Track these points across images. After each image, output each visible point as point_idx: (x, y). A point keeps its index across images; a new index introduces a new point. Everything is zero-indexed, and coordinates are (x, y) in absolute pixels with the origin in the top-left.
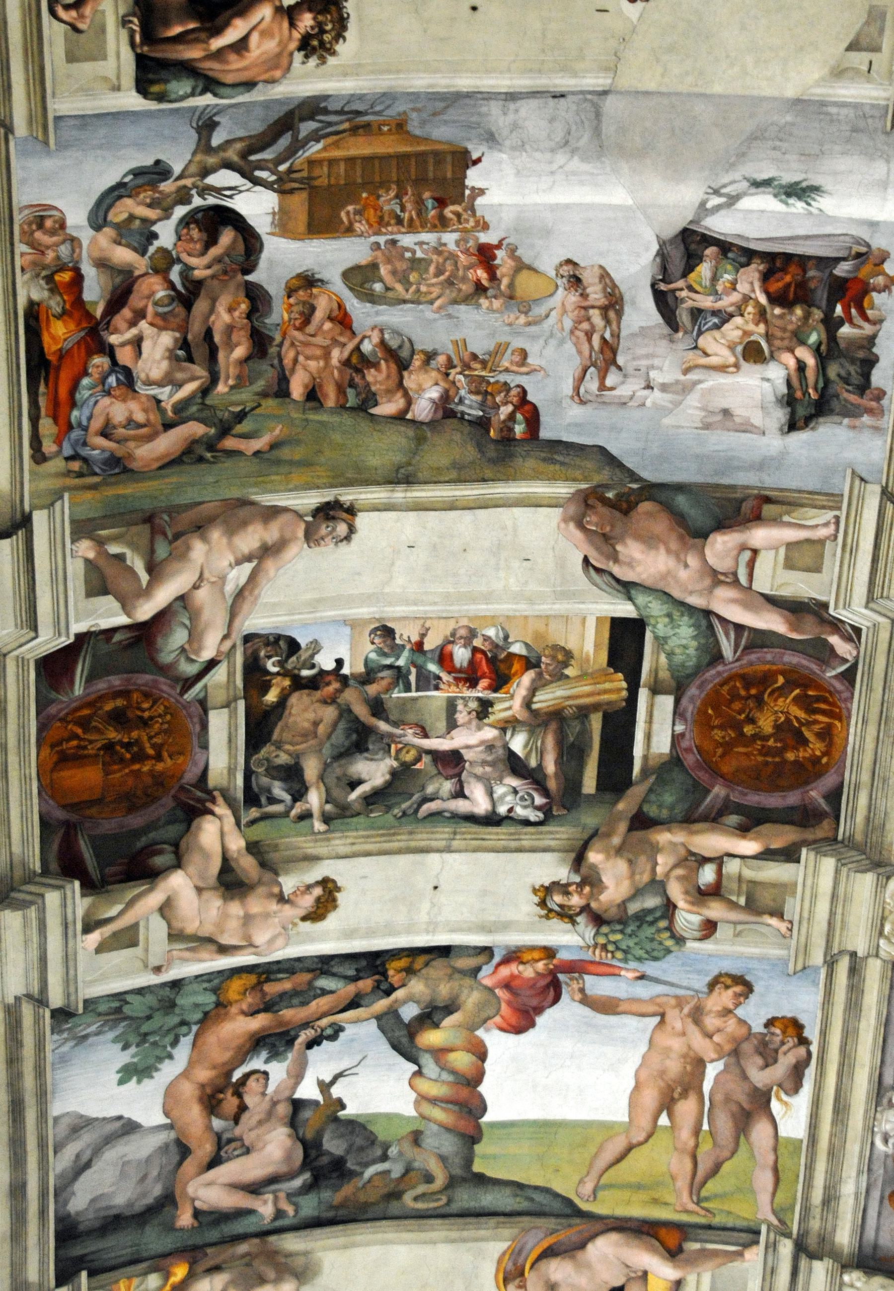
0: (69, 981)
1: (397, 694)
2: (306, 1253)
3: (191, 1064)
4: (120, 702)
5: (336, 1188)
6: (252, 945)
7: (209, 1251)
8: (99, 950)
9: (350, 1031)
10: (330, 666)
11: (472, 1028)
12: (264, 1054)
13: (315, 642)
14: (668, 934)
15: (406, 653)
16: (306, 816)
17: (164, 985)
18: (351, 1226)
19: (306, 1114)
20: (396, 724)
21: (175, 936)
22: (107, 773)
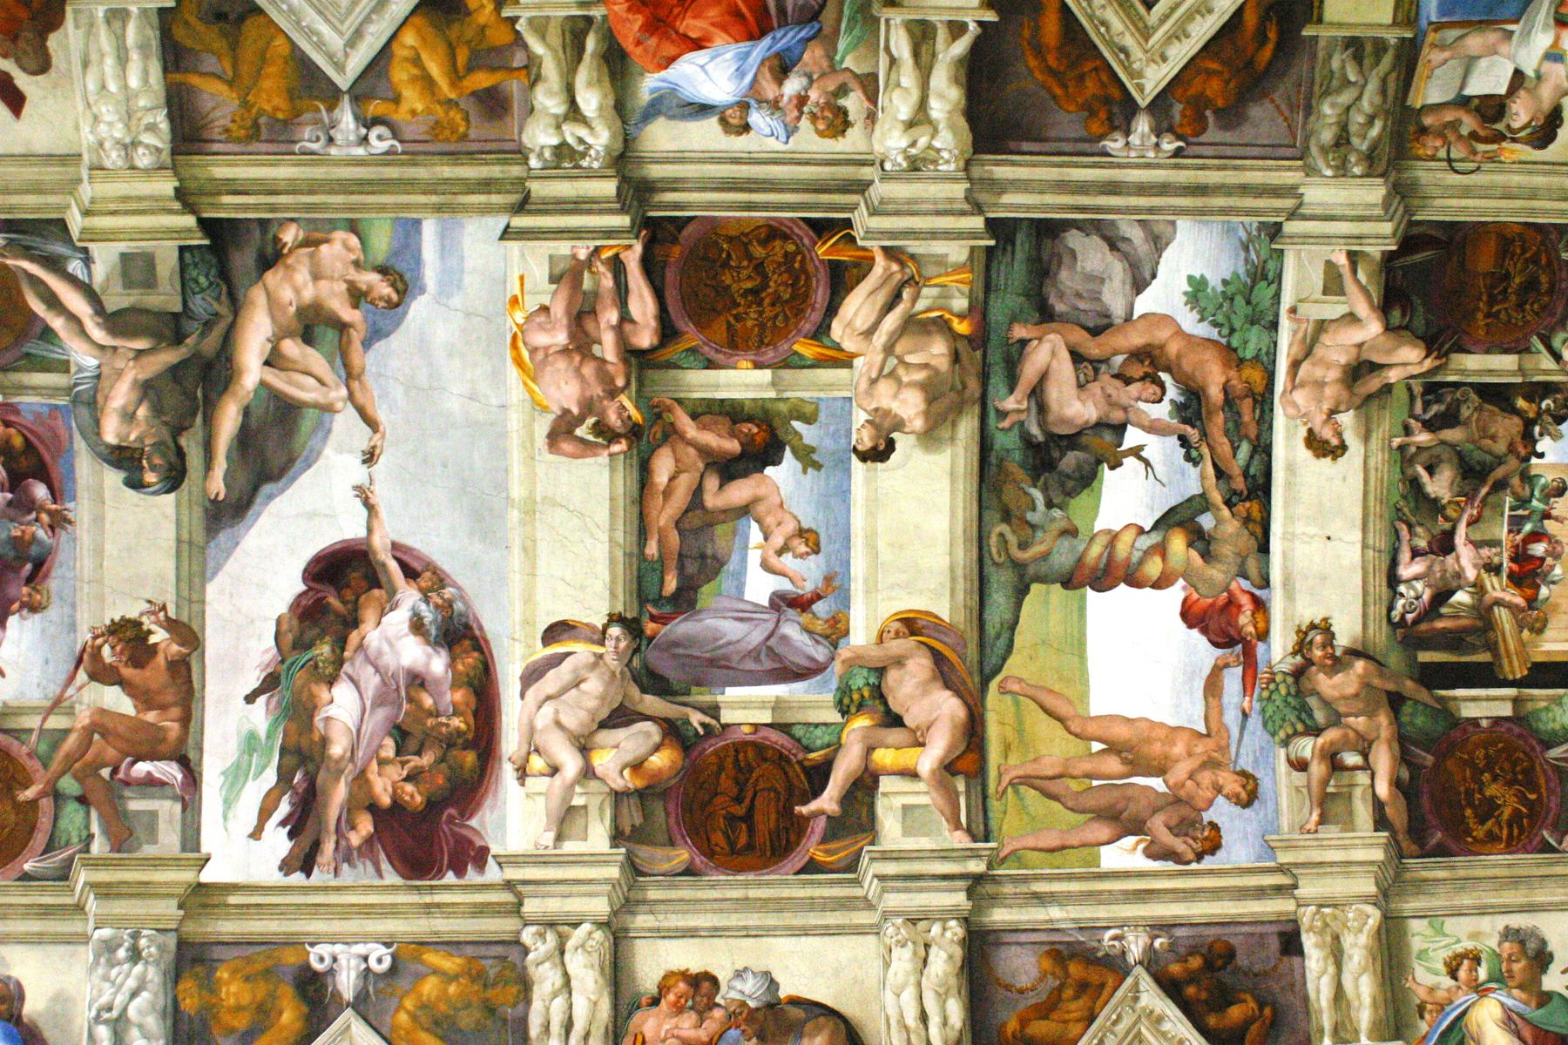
0: (1306, 238)
1: (1509, 500)
2: (953, 439)
3: (1189, 337)
4: (1545, 287)
5: (1022, 465)
6: (1294, 388)
7: (979, 354)
8: (1330, 265)
9: (1193, 471)
10: (1539, 448)
12: (1181, 399)
13: (1562, 436)
14: (1290, 731)
15: (1541, 506)
16: (1407, 431)
17: (1277, 315)
18: (976, 478)
19: (1108, 437)
20: (1484, 501)
21: (1321, 326)
22: (1485, 275)
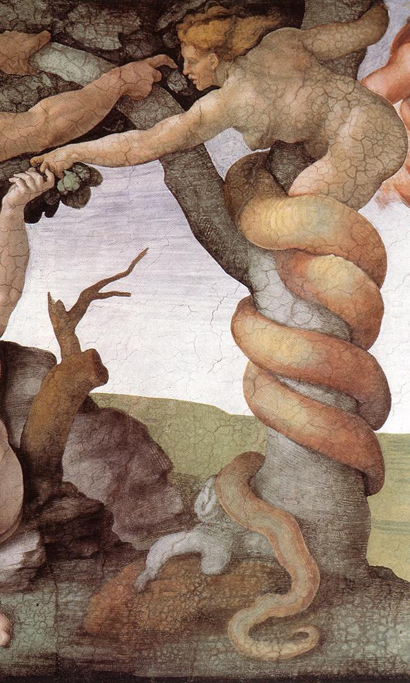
9: (112, 183)
11: (355, 201)
